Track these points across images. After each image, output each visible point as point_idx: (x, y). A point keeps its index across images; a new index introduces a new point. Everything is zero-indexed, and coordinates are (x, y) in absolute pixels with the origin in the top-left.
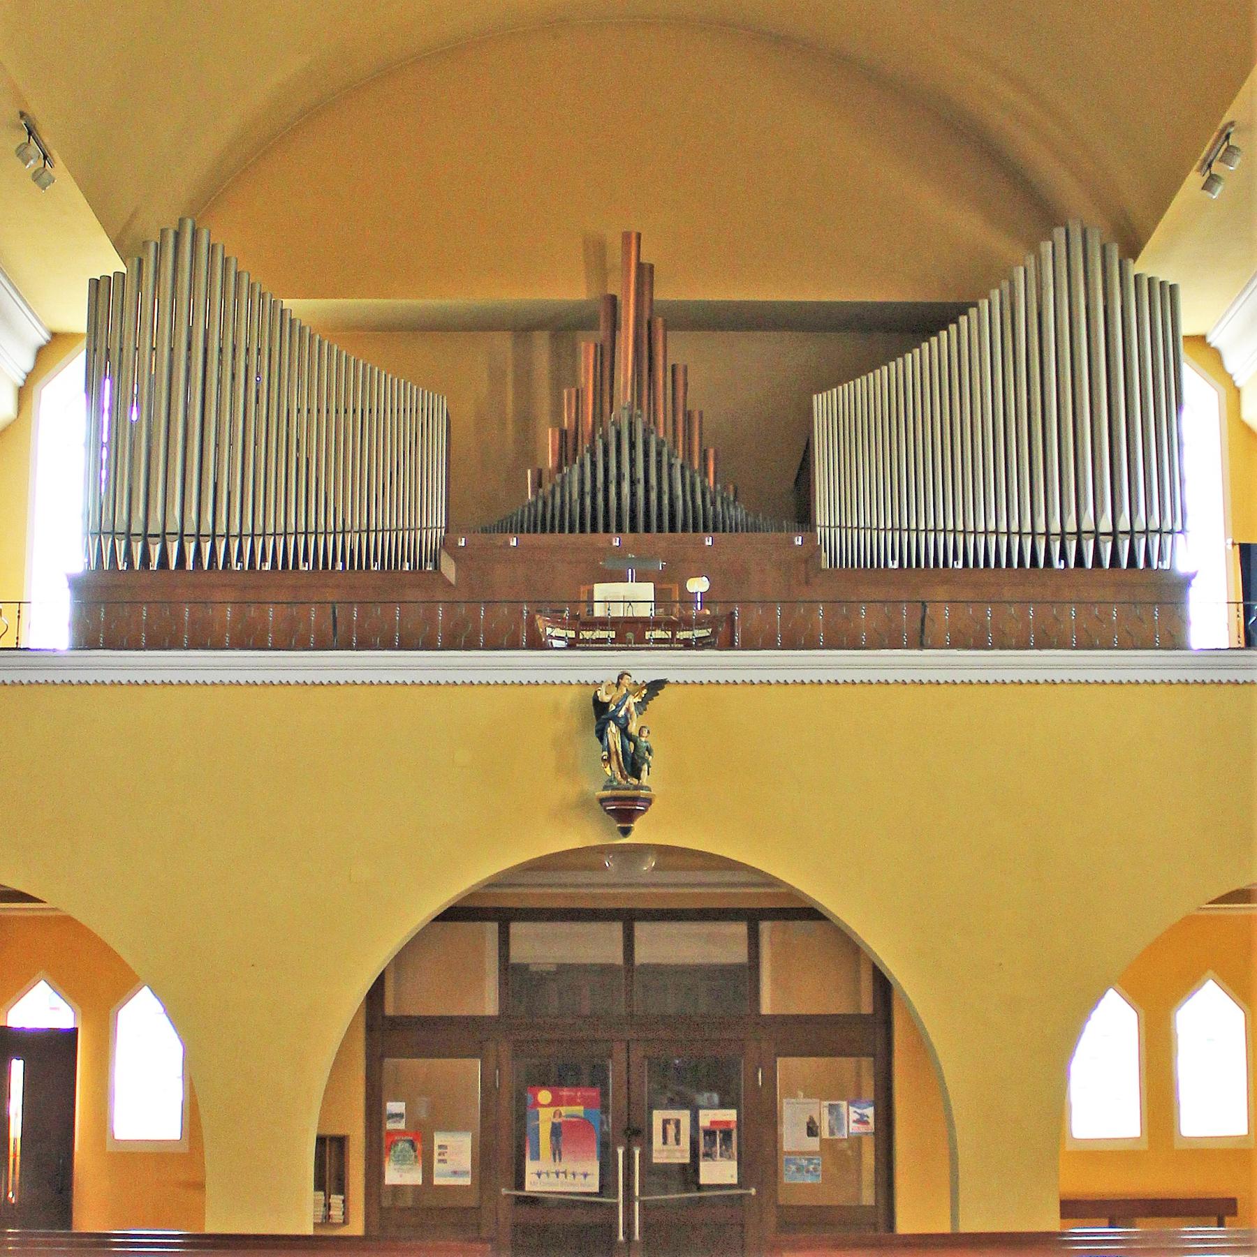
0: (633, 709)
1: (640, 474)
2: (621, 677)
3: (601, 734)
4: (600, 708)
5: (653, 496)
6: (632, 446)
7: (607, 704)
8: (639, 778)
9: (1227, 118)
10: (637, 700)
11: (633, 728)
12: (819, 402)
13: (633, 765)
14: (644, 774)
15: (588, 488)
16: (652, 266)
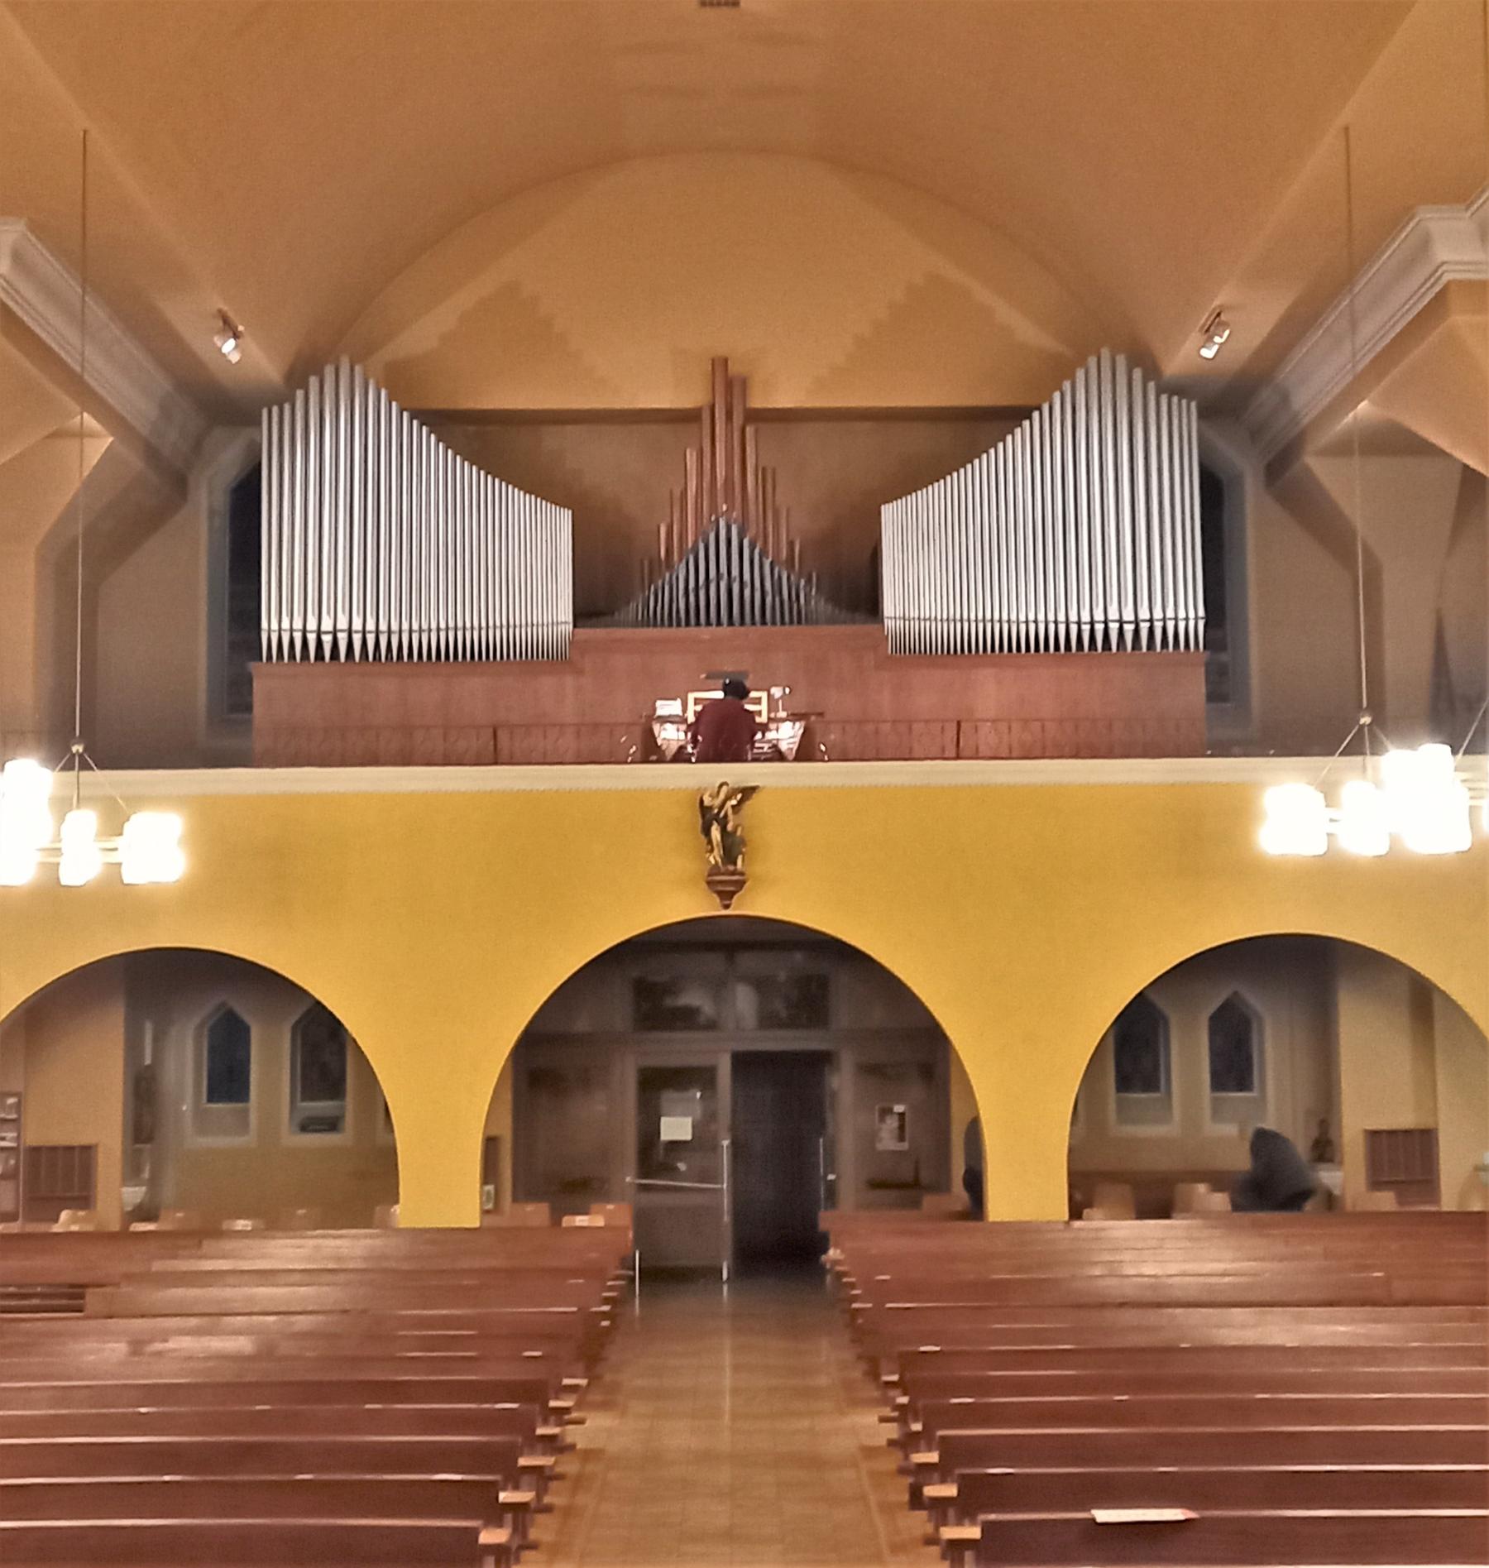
0: (730, 812)
1: (735, 572)
2: (721, 786)
3: (707, 831)
4: (704, 810)
5: (747, 592)
7: (711, 808)
8: (735, 864)
9: (1217, 303)
10: (734, 802)
11: (730, 827)
12: (888, 512)
13: (729, 855)
16: (744, 383)
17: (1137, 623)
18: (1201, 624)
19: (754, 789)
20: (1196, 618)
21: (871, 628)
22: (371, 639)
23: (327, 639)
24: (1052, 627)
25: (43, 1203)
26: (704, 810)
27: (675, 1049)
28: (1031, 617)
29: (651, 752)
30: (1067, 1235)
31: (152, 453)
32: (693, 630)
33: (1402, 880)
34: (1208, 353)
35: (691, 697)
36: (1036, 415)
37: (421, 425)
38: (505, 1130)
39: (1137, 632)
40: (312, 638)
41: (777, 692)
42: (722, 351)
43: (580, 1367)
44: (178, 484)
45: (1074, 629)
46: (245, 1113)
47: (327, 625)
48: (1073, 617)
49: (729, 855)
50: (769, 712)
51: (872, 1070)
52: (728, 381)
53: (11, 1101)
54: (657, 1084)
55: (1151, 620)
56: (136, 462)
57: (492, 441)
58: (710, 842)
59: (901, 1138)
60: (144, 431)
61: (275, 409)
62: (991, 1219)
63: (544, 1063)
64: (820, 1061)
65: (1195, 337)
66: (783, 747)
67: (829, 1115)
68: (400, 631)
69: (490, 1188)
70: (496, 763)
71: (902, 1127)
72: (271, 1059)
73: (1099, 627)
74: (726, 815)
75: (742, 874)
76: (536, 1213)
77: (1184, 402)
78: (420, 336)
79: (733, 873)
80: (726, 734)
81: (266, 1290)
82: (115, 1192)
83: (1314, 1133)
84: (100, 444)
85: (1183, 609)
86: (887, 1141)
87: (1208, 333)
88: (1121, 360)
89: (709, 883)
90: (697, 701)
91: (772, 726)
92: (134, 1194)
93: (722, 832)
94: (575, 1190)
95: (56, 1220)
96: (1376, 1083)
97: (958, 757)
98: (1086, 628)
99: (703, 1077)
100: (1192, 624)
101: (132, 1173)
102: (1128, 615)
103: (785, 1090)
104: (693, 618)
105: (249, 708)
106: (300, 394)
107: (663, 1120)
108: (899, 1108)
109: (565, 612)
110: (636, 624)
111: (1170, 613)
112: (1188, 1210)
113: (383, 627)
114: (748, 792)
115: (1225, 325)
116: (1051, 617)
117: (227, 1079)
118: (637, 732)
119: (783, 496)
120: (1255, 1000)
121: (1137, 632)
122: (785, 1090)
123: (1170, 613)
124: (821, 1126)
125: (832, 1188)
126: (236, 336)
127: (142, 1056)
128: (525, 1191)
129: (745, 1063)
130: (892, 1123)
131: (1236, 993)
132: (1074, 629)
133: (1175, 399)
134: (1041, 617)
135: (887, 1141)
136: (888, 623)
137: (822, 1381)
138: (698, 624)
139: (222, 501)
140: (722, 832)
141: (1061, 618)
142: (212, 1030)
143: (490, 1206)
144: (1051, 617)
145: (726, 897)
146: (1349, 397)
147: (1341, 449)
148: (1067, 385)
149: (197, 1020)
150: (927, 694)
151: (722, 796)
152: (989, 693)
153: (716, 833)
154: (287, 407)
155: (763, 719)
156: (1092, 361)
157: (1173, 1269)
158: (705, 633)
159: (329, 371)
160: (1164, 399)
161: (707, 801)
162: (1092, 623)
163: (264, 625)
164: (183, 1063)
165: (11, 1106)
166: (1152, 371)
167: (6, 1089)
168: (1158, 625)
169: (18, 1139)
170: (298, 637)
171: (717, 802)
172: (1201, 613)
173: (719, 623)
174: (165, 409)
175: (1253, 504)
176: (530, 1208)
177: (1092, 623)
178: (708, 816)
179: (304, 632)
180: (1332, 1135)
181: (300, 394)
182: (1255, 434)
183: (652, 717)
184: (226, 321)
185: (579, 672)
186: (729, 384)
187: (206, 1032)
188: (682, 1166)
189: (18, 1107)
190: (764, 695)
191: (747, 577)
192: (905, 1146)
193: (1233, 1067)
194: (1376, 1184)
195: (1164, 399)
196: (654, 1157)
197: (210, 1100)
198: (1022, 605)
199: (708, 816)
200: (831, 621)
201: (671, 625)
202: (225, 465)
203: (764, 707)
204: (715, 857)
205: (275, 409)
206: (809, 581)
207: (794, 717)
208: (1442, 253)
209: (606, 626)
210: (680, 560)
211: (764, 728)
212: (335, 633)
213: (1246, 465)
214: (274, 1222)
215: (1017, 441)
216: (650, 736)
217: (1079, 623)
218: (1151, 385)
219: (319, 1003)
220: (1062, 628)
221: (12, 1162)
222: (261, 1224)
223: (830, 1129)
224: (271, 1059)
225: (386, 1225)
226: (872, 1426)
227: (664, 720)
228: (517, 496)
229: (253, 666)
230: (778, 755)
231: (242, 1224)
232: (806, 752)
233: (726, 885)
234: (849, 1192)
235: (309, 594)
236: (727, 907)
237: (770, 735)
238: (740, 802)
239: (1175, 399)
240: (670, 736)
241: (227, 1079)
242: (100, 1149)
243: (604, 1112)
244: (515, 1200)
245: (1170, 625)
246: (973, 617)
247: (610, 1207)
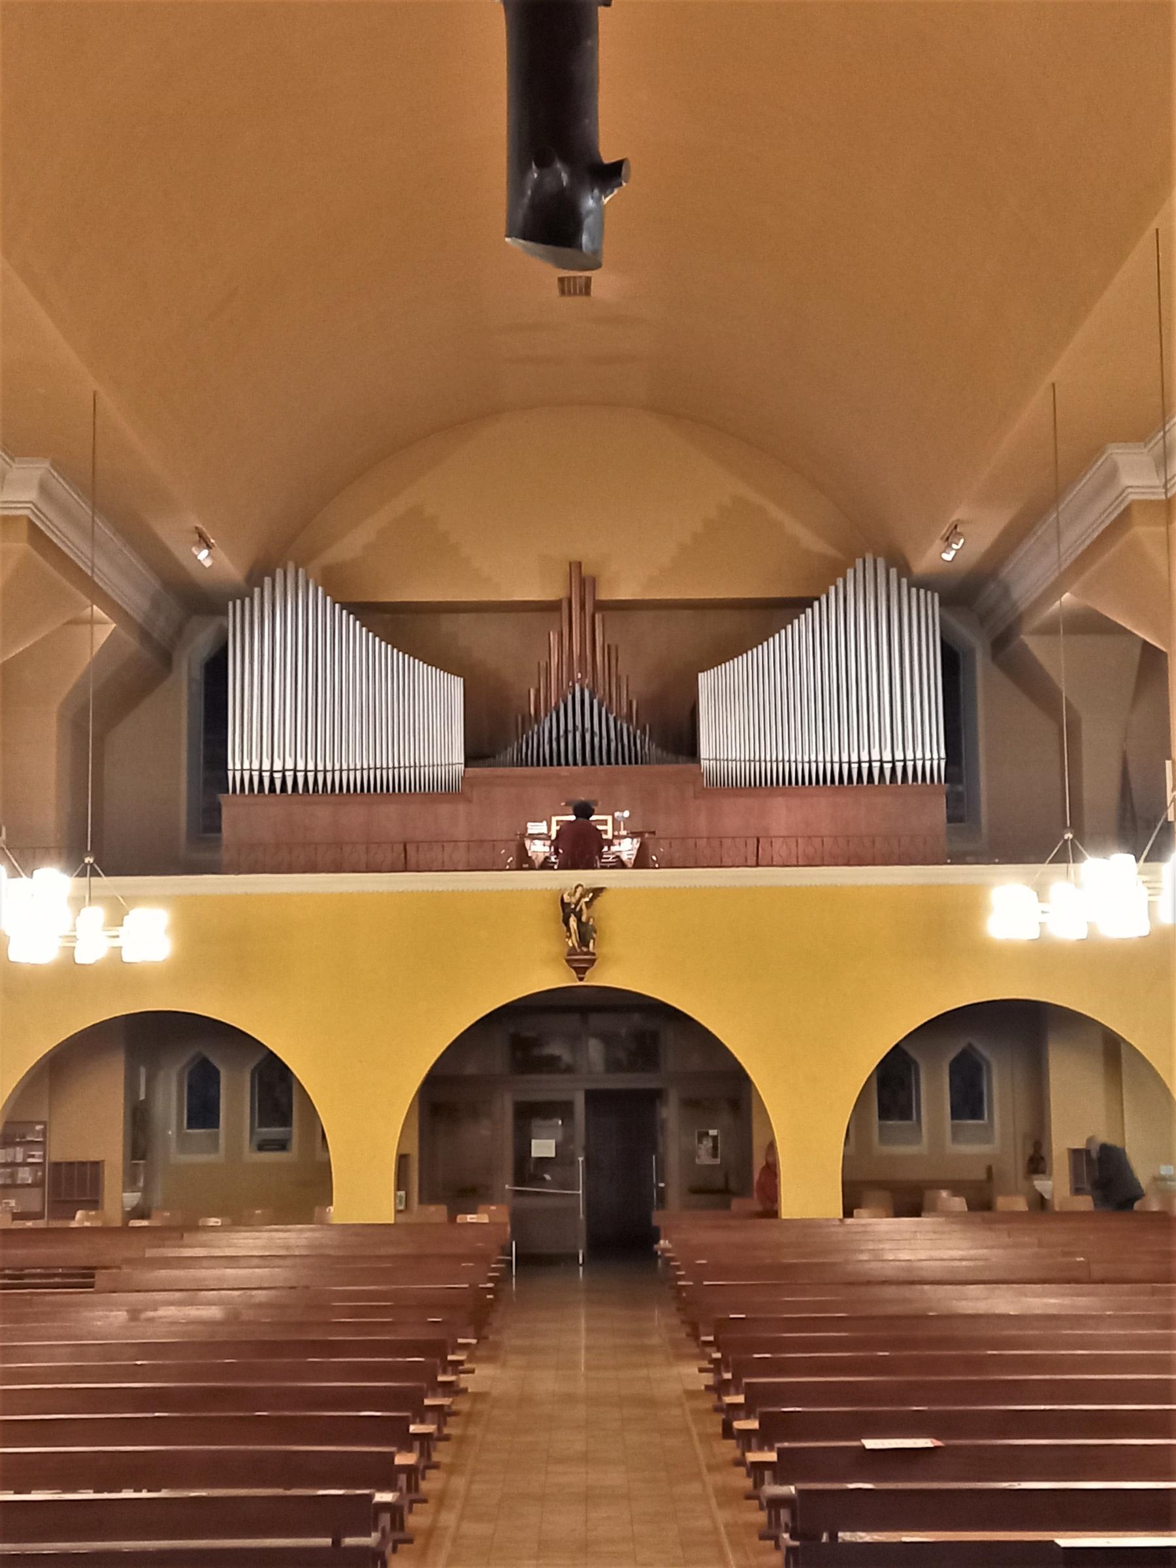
0: (584, 907)
3: (566, 922)
4: (564, 904)
5: (596, 740)
7: (569, 904)
8: (588, 946)
9: (954, 518)
10: (587, 899)
11: (584, 919)
13: (584, 940)
14: (591, 945)
16: (594, 581)
17: (893, 762)
19: (601, 890)
20: (939, 759)
21: (691, 765)
22: (311, 776)
23: (278, 776)
24: (829, 766)
25: (63, 1205)
26: (564, 904)
27: (544, 1088)
28: (813, 758)
29: (524, 862)
30: (841, 1230)
31: (144, 635)
32: (556, 769)
33: (1096, 958)
34: (948, 557)
35: (554, 819)
36: (816, 604)
37: (349, 614)
38: (414, 1151)
39: (893, 769)
40: (266, 775)
42: (575, 557)
43: (471, 1330)
44: (165, 658)
45: (845, 767)
46: (216, 1137)
47: (278, 766)
48: (845, 758)
49: (584, 940)
50: (614, 830)
51: (691, 1104)
52: (582, 579)
53: (38, 1127)
54: (529, 1115)
55: (905, 761)
56: (132, 643)
57: (404, 627)
58: (569, 930)
59: (715, 1156)
60: (139, 620)
61: (238, 602)
62: (784, 1217)
63: (443, 1099)
64: (653, 1097)
65: (938, 544)
66: (624, 857)
67: (660, 1139)
68: (333, 771)
69: (402, 1193)
70: (405, 870)
71: (715, 1147)
72: (236, 1096)
73: (865, 766)
74: (581, 909)
75: (593, 954)
76: (437, 1213)
77: (929, 593)
78: (350, 546)
79: (588, 953)
80: (580, 847)
81: (229, 1272)
82: (118, 1197)
83: (1030, 1151)
84: (105, 629)
85: (929, 752)
86: (704, 1157)
87: (948, 541)
88: (881, 563)
89: (568, 961)
90: (558, 822)
91: (616, 841)
92: (132, 1198)
93: (578, 923)
94: (466, 1195)
95: (73, 1218)
96: (1078, 1113)
97: (757, 865)
98: (855, 766)
99: (563, 1109)
100: (935, 763)
101: (130, 1182)
102: (887, 756)
103: (625, 1121)
104: (555, 760)
105: (219, 829)
106: (257, 590)
107: (533, 1142)
108: (713, 1132)
109: (459, 756)
110: (512, 765)
111: (919, 755)
112: (934, 1210)
113: (320, 767)
114: (597, 892)
115: (961, 535)
116: (828, 758)
117: (203, 1112)
118: (513, 846)
119: (624, 666)
120: (984, 1050)
121: (893, 769)
122: (625, 1121)
123: (919, 755)
124: (654, 1148)
125: (662, 1193)
127: (138, 1095)
128: (428, 1196)
129: (594, 1098)
130: (708, 1144)
131: (970, 1045)
132: (845, 767)
133: (922, 592)
134: (820, 758)
135: (704, 1157)
137: (655, 1340)
138: (559, 764)
139: (198, 674)
140: (578, 923)
141: (836, 759)
142: (191, 1073)
143: (402, 1207)
144: (828, 758)
145: (581, 972)
146: (1055, 590)
147: (1050, 629)
148: (840, 582)
149: (178, 1067)
150: (734, 817)
151: (578, 895)
152: (781, 816)
153: (573, 922)
154: (247, 600)
155: (609, 836)
156: (859, 562)
157: (922, 1255)
158: (564, 770)
159: (279, 573)
160: (914, 590)
161: (566, 899)
162: (859, 762)
163: (230, 766)
164: (169, 1100)
165: (38, 1132)
166: (904, 570)
167: (36, 1119)
168: (910, 764)
169: (44, 1157)
170: (256, 774)
171: (574, 900)
172: (943, 755)
173: (575, 764)
174: (156, 604)
175: (983, 670)
176: (432, 1208)
177: (859, 762)
178: (567, 910)
179: (261, 771)
180: (1044, 1152)
181: (257, 590)
182: (983, 619)
183: (524, 835)
184: (201, 536)
185: (469, 801)
186: (582, 582)
187: (186, 1074)
188: (548, 1177)
189: (44, 1133)
190: (609, 818)
192: (718, 1161)
193: (968, 1101)
194: (1077, 1191)
195: (914, 590)
196: (527, 1171)
197: (190, 1126)
198: (807, 750)
199: (567, 910)
200: (660, 761)
201: (538, 765)
202: (200, 645)
203: (609, 827)
204: (573, 942)
205: (238, 602)
206: (643, 732)
207: (633, 835)
208: (1126, 480)
209: (490, 766)
210: (546, 715)
211: (610, 843)
212: (284, 771)
213: (977, 640)
214: (238, 1220)
215: (802, 623)
216: (523, 850)
217: (850, 763)
218: (904, 581)
219: (271, 1052)
220: (836, 767)
221: (40, 1174)
222: (228, 1221)
223: (661, 1150)
224: (236, 1096)
225: (323, 1222)
226: (693, 1375)
227: (534, 837)
228: (421, 667)
229: (222, 798)
230: (620, 864)
231: (213, 1221)
232: (641, 862)
233: (581, 962)
234: (674, 1196)
235: (264, 741)
236: (581, 979)
237: (613, 849)
238: (592, 900)
239: (922, 592)
240: (538, 849)
241: (203, 1112)
242: (106, 1163)
243: (489, 1134)
244: (421, 1202)
245: (919, 764)
246: (768, 758)
247: (493, 1208)
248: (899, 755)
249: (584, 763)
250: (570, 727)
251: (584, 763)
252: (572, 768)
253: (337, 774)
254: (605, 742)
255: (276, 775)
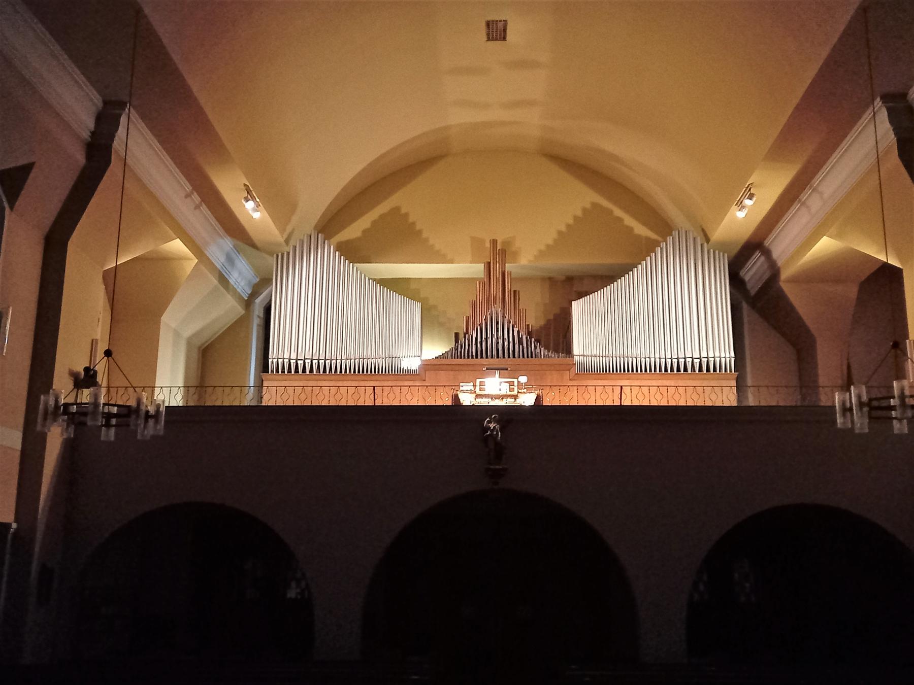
5: (506, 343)
6: (497, 323)
15: (479, 340)
18: (733, 360)
24: (658, 360)
41: (523, 379)
65: (734, 207)
91: (520, 395)
126: (253, 199)
132: (669, 361)
136: (576, 358)
144: (657, 356)
155: (515, 392)
158: (484, 361)
172: (733, 354)
191: (506, 336)
210: (473, 329)
227: (463, 391)
248: (704, 354)
249: (498, 357)
250: (489, 335)
251: (498, 357)
252: (490, 359)
253: (339, 361)
254: (511, 345)
255: (299, 362)
